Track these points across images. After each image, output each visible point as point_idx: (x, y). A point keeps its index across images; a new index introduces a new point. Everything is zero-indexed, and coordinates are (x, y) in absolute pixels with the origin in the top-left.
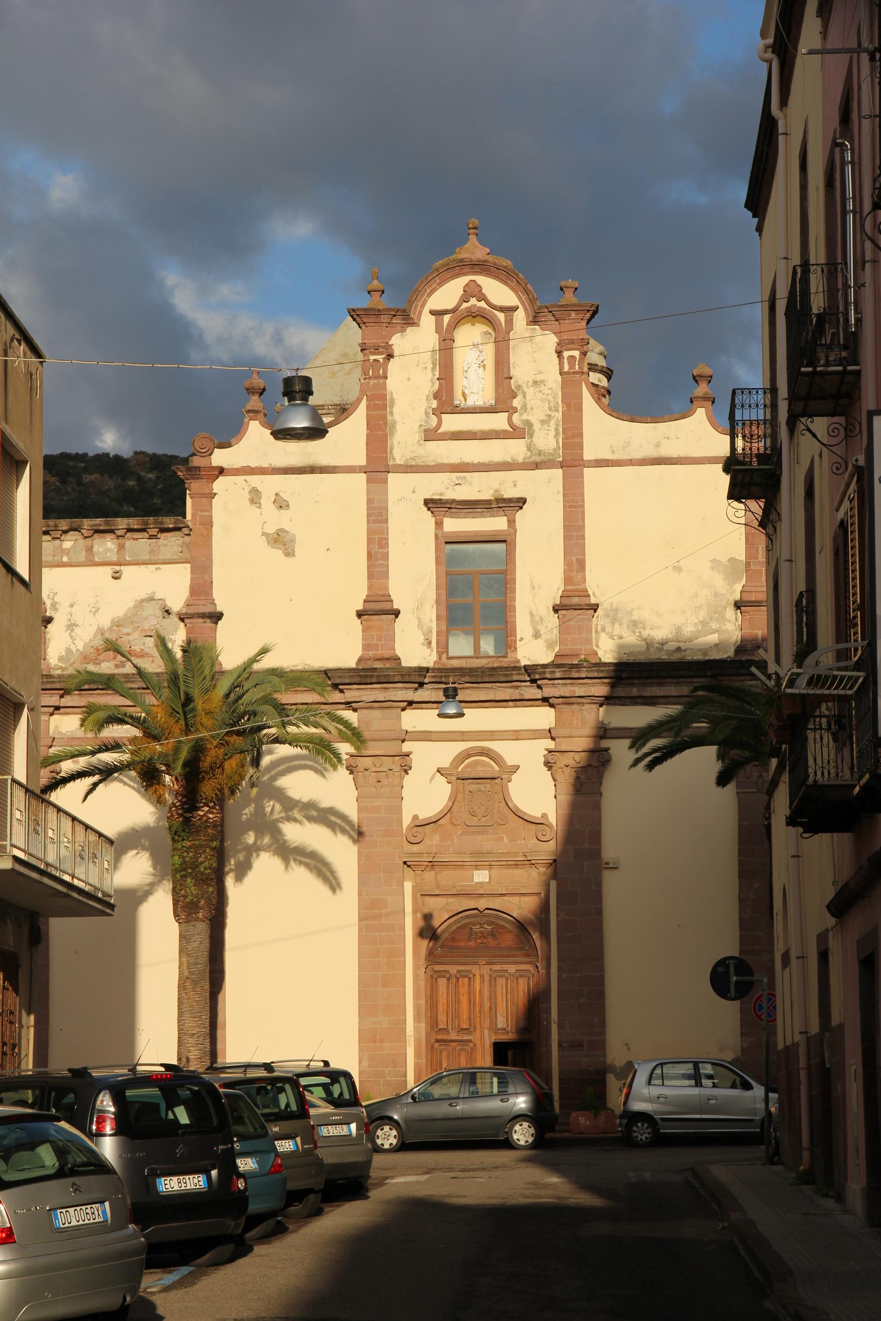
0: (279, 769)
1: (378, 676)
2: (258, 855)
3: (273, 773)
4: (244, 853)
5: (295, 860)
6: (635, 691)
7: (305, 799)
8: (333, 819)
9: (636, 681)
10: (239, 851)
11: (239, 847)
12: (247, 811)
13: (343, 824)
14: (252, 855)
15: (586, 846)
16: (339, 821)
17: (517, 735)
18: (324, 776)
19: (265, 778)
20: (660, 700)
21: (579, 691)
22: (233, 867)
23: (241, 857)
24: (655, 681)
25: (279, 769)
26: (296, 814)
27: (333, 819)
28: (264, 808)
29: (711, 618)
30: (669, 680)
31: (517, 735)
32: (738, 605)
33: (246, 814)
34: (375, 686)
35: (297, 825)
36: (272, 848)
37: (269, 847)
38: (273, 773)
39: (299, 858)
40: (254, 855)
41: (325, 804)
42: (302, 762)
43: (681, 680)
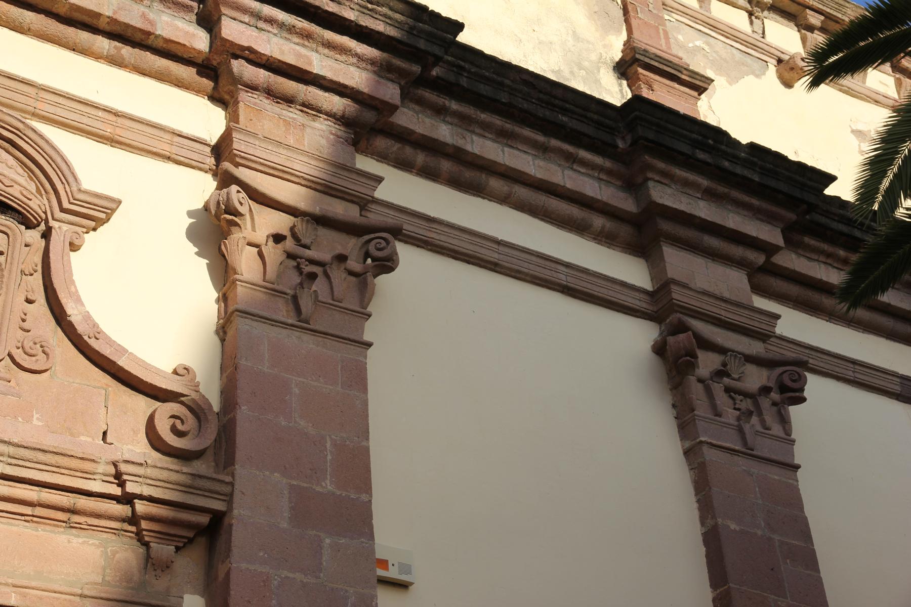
6: (444, 132)
9: (454, 106)
15: (328, 486)
17: (115, 130)
20: (495, 183)
21: (319, 63)
24: (497, 121)
29: (572, 73)
30: (527, 132)
31: (115, 130)
32: (625, 68)
43: (555, 143)
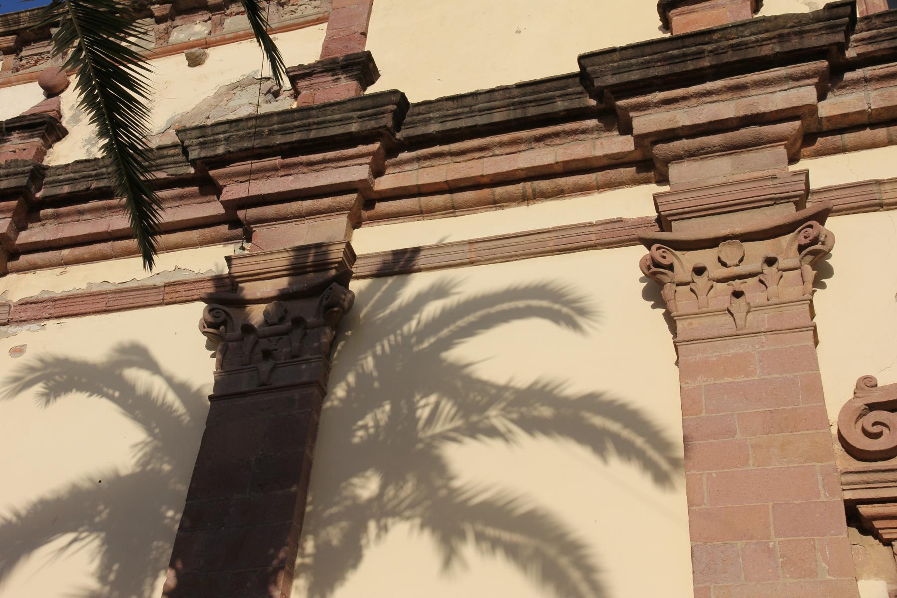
0: (461, 323)
1: (714, 52)
2: (383, 529)
3: (445, 332)
4: (344, 524)
5: (480, 537)
7: (523, 381)
8: (598, 421)
10: (331, 521)
11: (334, 510)
12: (369, 420)
13: (626, 433)
14: (364, 528)
16: (615, 427)
18: (574, 325)
19: (426, 344)
22: (308, 560)
23: (334, 534)
25: (461, 323)
26: (495, 417)
27: (598, 421)
28: (413, 408)
33: (365, 427)
34: (709, 86)
35: (497, 444)
36: (419, 510)
37: (412, 506)
38: (445, 332)
39: (491, 532)
40: (372, 526)
41: (576, 387)
42: (521, 304)
